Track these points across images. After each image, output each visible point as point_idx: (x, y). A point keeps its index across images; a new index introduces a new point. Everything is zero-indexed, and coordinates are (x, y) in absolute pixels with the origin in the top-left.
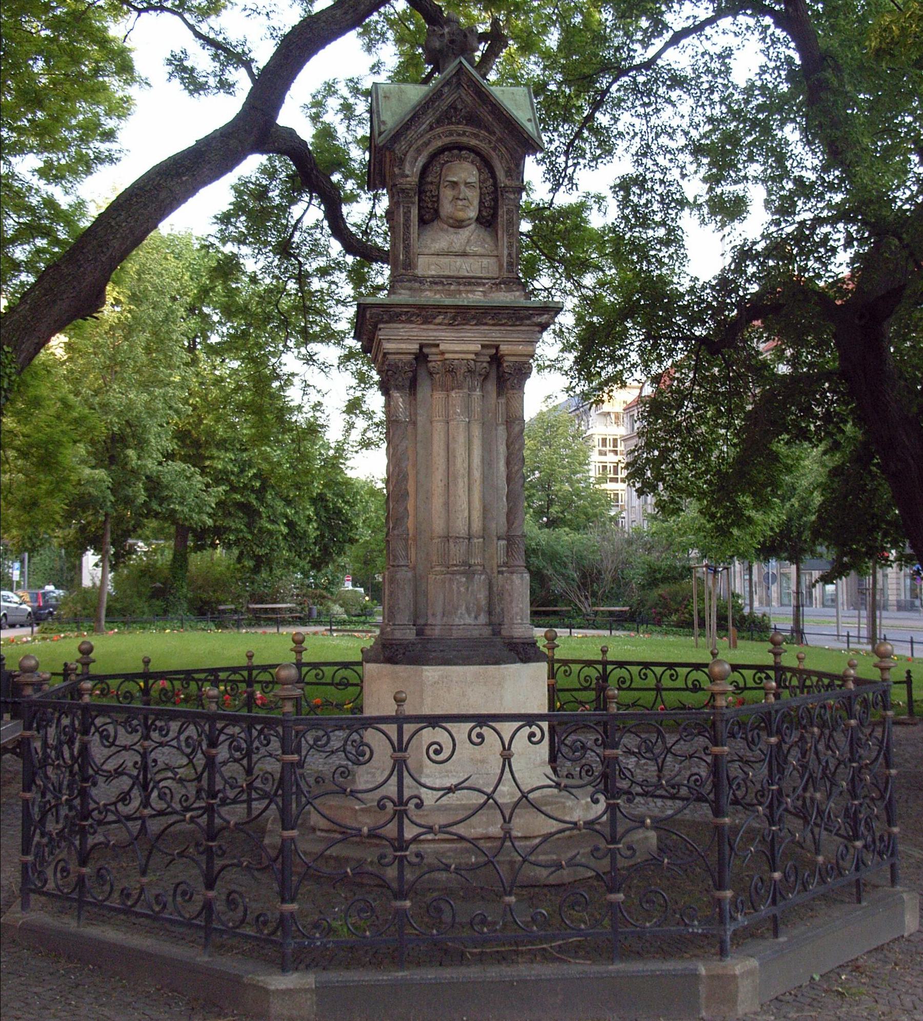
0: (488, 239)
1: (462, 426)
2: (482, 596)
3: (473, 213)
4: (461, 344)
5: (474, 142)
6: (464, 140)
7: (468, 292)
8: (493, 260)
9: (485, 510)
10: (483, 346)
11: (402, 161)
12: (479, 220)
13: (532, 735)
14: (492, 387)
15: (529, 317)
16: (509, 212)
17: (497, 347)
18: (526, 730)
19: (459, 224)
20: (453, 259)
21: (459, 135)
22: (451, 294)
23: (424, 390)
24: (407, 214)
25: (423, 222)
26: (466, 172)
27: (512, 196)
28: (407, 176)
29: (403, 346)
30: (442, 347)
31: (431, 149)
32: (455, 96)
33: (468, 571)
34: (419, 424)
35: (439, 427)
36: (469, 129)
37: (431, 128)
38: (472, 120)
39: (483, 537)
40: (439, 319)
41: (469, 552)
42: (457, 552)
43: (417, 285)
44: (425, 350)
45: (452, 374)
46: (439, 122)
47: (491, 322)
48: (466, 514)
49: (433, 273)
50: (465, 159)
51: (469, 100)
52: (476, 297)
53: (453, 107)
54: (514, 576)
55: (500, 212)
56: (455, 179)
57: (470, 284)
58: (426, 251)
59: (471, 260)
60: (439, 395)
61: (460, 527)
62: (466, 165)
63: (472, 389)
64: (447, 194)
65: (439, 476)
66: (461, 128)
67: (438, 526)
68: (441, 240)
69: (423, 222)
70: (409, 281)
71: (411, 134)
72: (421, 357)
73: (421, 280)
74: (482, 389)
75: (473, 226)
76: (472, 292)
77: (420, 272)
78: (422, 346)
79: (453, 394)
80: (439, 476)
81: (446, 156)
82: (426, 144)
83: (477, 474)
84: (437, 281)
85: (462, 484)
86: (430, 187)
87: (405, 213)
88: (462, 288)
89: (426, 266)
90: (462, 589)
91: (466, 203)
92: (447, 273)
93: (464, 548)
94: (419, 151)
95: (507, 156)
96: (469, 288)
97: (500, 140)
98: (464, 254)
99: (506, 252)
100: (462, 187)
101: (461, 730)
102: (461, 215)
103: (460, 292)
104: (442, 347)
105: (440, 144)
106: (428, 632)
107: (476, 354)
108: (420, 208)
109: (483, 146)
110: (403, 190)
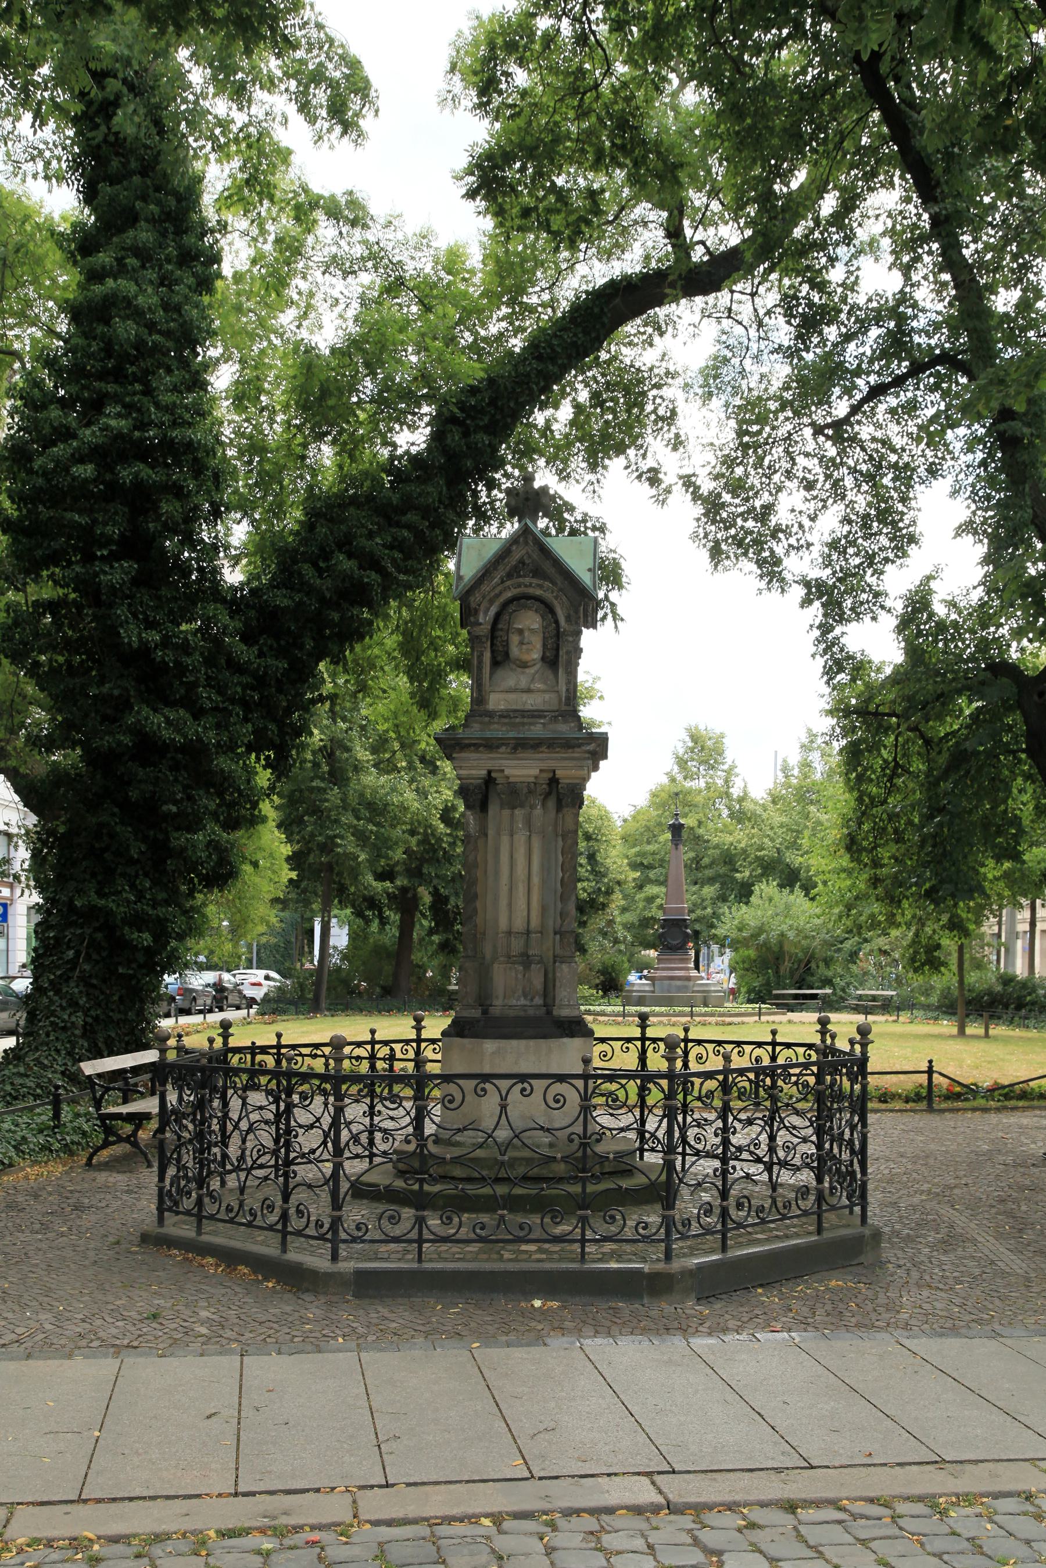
0: (551, 677)
1: (523, 839)
2: (538, 982)
3: (536, 655)
4: (522, 770)
5: (538, 592)
8: (553, 695)
9: (544, 909)
12: (543, 659)
13: (523, 1090)
14: (551, 804)
15: (579, 746)
16: (568, 653)
18: (520, 1086)
19: (524, 665)
23: (493, 809)
24: (480, 656)
25: (496, 664)
26: (530, 621)
33: (526, 960)
35: (505, 839)
36: (535, 581)
38: (537, 573)
40: (503, 749)
41: (527, 945)
42: (517, 946)
45: (516, 796)
46: (509, 576)
52: (537, 730)
53: (521, 562)
60: (506, 812)
61: (519, 924)
63: (533, 807)
64: (515, 639)
65: (504, 879)
66: (527, 580)
67: (503, 924)
68: (510, 678)
69: (496, 664)
71: (485, 588)
72: (489, 780)
73: (490, 714)
74: (543, 805)
77: (491, 706)
78: (489, 772)
79: (517, 812)
80: (504, 879)
81: (512, 608)
82: (498, 596)
83: (536, 880)
84: (506, 715)
89: (496, 701)
93: (522, 942)
94: (491, 602)
98: (529, 691)
101: (469, 1085)
102: (525, 657)
106: (492, 1009)
108: (493, 652)
109: (548, 596)
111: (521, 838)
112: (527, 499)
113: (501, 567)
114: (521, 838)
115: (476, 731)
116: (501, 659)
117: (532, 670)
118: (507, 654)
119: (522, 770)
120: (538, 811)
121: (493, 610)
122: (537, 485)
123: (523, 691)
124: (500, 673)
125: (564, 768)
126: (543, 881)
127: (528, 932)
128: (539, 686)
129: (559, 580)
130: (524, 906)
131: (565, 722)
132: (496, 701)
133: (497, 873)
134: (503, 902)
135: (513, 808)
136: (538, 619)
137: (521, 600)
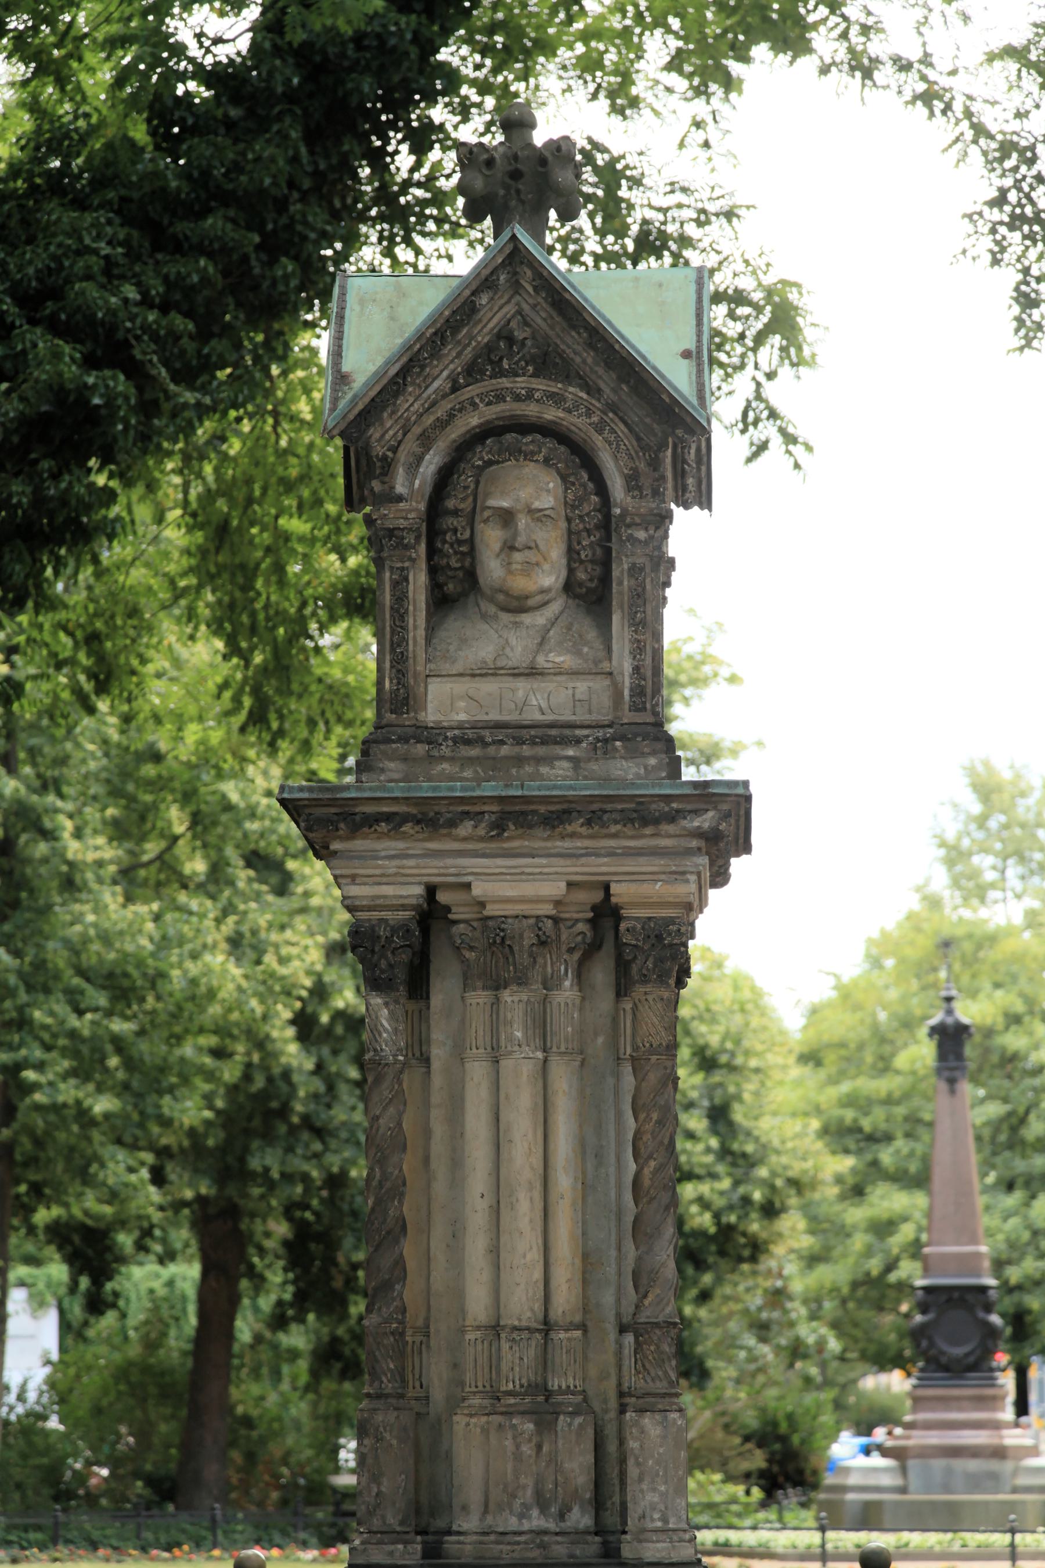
0: (592, 634)
2: (577, 1466)
3: (549, 577)
4: (520, 883)
5: (551, 414)
6: (531, 410)
7: (538, 760)
8: (601, 684)
9: (588, 1262)
10: (570, 884)
11: (387, 466)
12: (569, 587)
14: (602, 973)
15: (672, 818)
16: (635, 570)
17: (607, 887)
19: (518, 605)
20: (509, 683)
21: (517, 398)
22: (495, 766)
23: (443, 989)
24: (400, 583)
25: (442, 602)
26: (531, 489)
27: (641, 535)
28: (400, 499)
29: (388, 890)
30: (479, 889)
31: (456, 431)
32: (510, 309)
33: (542, 1405)
34: (436, 1065)
35: (477, 1072)
36: (541, 385)
37: (455, 388)
38: (547, 362)
39: (583, 1327)
40: (465, 829)
41: (544, 1361)
42: (517, 1363)
43: (421, 749)
44: (442, 897)
45: (502, 953)
46: (472, 372)
47: (583, 830)
48: (538, 1274)
49: (462, 717)
50: (529, 456)
51: (538, 320)
52: (557, 777)
53: (505, 335)
54: (647, 1420)
55: (615, 573)
56: (505, 504)
57: (545, 741)
58: (446, 668)
59: (549, 685)
60: (479, 998)
61: (521, 1305)
62: (531, 469)
63: (549, 984)
64: (491, 537)
65: (478, 1182)
66: (521, 383)
68: (479, 639)
69: (442, 602)
70: (404, 739)
71: (409, 404)
72: (431, 913)
75: (555, 607)
76: (549, 760)
77: (431, 715)
78: (431, 891)
80: (478, 1182)
81: (482, 454)
83: (564, 1182)
84: (469, 735)
85: (524, 1210)
86: (451, 522)
87: (395, 584)
88: (526, 750)
89: (445, 702)
90: (527, 1449)
91: (532, 556)
92: (494, 716)
93: (531, 1353)
94: (426, 441)
95: (629, 442)
96: (541, 751)
97: (612, 407)
98: (532, 672)
99: (627, 667)
100: (522, 522)
102: (520, 584)
103: (519, 761)
104: (479, 889)
105: (474, 421)
107: (558, 903)
108: (433, 571)
109: (577, 423)
110: (391, 532)
111: (520, 1067)
112: (516, 175)
113: (450, 351)
114: (520, 1067)
115: (392, 781)
116: (456, 589)
117: (540, 619)
118: (471, 577)
119: (520, 883)
120: (567, 992)
121: (431, 463)
122: (539, 138)
123: (516, 674)
124: (454, 626)
125: (633, 877)
126: (586, 1187)
127: (547, 1326)
128: (563, 659)
129: (606, 380)
130: (535, 1255)
131: (633, 754)
132: (445, 702)
133: (457, 1162)
134: (476, 1246)
135: (497, 985)
136: (553, 483)
137: (507, 435)
